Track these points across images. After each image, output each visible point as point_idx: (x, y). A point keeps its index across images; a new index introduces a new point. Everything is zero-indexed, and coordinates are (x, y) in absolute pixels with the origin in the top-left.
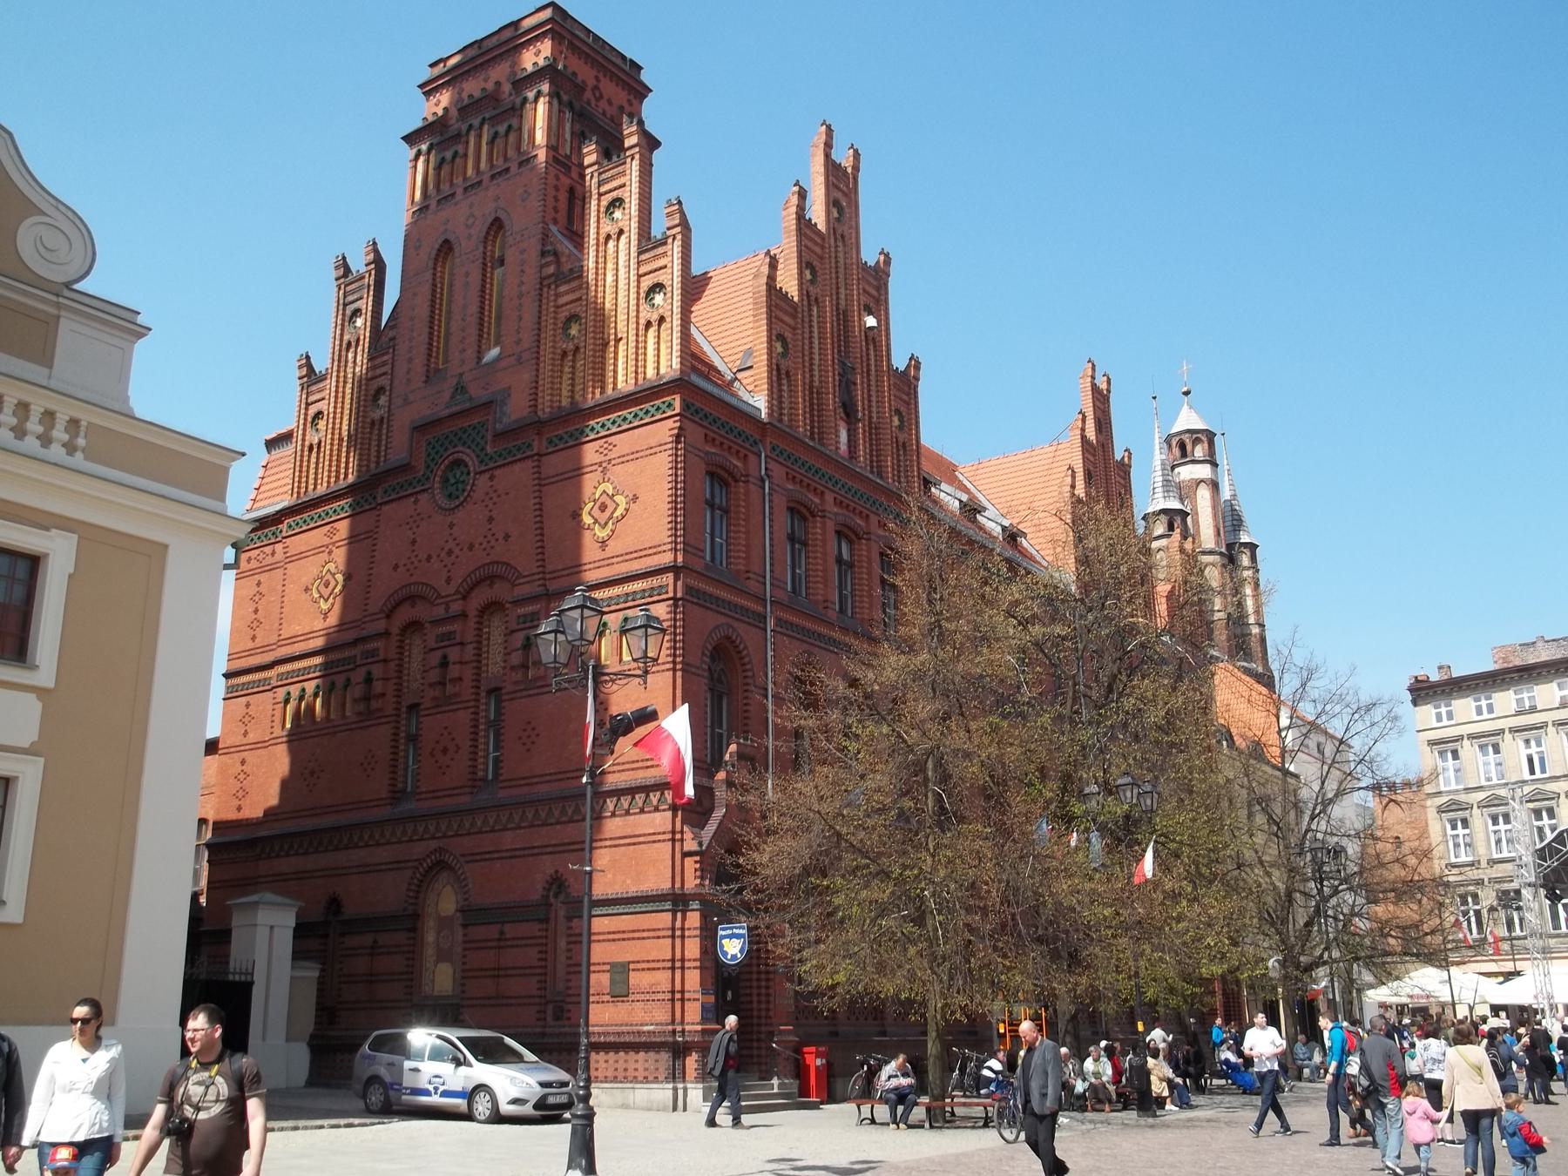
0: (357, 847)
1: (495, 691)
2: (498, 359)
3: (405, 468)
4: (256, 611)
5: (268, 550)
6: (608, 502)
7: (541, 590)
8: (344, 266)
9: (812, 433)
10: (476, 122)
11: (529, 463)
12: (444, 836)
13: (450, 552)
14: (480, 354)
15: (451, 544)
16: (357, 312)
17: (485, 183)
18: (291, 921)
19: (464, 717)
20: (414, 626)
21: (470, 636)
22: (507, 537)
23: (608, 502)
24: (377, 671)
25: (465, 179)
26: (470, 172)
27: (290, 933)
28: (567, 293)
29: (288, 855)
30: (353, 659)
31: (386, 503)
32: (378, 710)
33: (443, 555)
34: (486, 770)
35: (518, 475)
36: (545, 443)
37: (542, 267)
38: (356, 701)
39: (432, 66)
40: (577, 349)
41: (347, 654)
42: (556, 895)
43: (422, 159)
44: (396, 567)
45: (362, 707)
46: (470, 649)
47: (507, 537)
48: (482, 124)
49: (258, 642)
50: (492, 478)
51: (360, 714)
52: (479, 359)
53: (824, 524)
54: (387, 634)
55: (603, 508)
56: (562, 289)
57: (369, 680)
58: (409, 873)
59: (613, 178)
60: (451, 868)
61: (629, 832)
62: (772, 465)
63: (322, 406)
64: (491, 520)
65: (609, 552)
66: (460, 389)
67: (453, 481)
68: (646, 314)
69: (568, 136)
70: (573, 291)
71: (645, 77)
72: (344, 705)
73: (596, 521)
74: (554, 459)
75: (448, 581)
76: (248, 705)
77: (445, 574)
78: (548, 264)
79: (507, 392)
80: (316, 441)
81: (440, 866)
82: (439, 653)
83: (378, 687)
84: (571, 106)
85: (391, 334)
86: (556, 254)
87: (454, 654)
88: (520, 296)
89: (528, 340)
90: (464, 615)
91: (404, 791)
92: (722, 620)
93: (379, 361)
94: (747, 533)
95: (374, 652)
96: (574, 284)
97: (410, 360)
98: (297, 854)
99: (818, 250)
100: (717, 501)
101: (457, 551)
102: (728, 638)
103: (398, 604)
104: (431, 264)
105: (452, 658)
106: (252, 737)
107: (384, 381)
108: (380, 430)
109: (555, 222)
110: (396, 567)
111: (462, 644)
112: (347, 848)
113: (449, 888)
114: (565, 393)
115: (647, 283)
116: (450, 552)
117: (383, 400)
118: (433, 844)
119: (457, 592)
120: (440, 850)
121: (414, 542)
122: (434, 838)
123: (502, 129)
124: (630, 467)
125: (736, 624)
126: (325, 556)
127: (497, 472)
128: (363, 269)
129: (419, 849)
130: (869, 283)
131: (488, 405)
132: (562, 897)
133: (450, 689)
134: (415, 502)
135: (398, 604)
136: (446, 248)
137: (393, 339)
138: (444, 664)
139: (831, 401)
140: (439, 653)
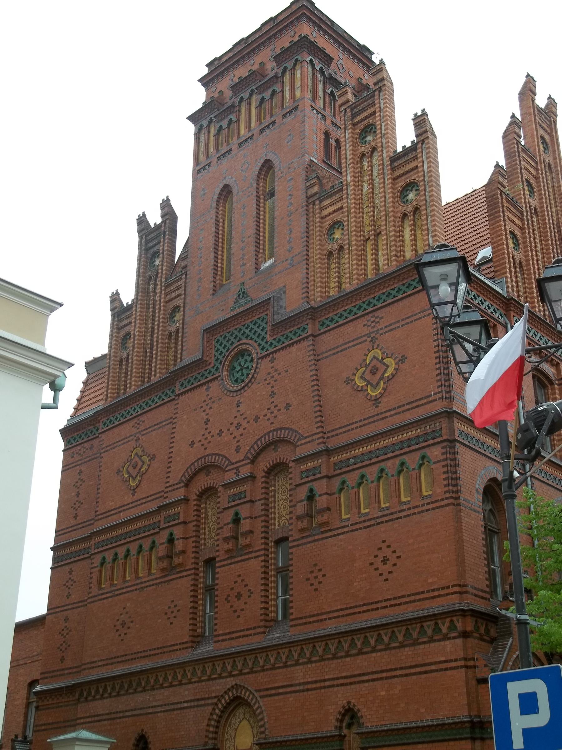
0: (162, 687)
2: (273, 266)
3: (199, 363)
4: (78, 494)
5: (87, 445)
6: (379, 365)
7: (322, 447)
10: (246, 95)
12: (241, 673)
13: (238, 426)
16: (156, 255)
19: (256, 565)
20: (208, 492)
21: (259, 494)
22: (288, 406)
23: (379, 365)
24: (178, 532)
26: (242, 132)
28: (330, 205)
29: (102, 698)
31: (182, 394)
32: (181, 565)
33: (233, 428)
34: (277, 612)
36: (318, 326)
37: (307, 188)
38: (160, 559)
40: (341, 248)
42: (349, 726)
43: (203, 132)
44: (193, 443)
45: (165, 564)
46: (259, 506)
47: (288, 406)
49: (79, 520)
51: (163, 570)
55: (374, 371)
56: (325, 203)
57: (171, 541)
60: (248, 704)
61: (420, 660)
63: (131, 328)
64: (273, 394)
65: (383, 407)
66: (243, 294)
67: (238, 368)
68: (402, 209)
72: (150, 564)
73: (368, 383)
74: (325, 338)
75: (237, 451)
76: (71, 572)
77: (234, 444)
79: (283, 291)
80: (125, 355)
81: (237, 702)
83: (179, 545)
85: (183, 264)
87: (244, 511)
91: (202, 636)
97: (200, 280)
98: (110, 696)
101: (244, 424)
103: (195, 474)
104: (214, 205)
105: (242, 515)
106: (74, 598)
107: (179, 301)
108: (176, 339)
110: (193, 443)
111: (251, 501)
112: (153, 689)
113: (245, 722)
114: (332, 285)
115: (401, 183)
116: (238, 426)
117: (178, 317)
118: (231, 682)
119: (246, 457)
120: (236, 686)
121: (207, 422)
122: (230, 675)
123: (267, 95)
126: (133, 443)
128: (159, 221)
131: (266, 303)
132: (355, 729)
133: (243, 541)
134: (207, 390)
135: (195, 474)
136: (226, 192)
137: (186, 267)
138: (237, 520)
140: (232, 512)
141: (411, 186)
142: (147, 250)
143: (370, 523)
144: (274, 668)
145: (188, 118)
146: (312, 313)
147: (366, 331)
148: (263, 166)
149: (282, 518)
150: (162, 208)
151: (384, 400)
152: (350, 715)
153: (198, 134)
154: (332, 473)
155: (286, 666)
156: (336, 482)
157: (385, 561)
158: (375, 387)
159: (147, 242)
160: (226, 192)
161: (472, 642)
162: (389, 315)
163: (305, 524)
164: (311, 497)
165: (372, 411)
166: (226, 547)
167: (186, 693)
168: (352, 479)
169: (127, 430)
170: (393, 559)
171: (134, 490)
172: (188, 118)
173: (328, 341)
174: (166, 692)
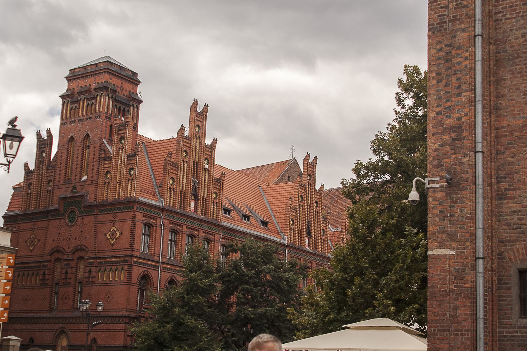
0: (39, 323)
1: (80, 283)
9: (180, 207)
11: (93, 217)
12: (64, 323)
14: (81, 178)
15: (70, 237)
16: (44, 151)
17: (85, 120)
18: (19, 344)
22: (86, 238)
25: (79, 117)
26: (80, 114)
27: (19, 348)
30: (39, 267)
31: (52, 220)
35: (90, 220)
39: (70, 70)
41: (38, 265)
42: (94, 343)
44: (53, 241)
45: (42, 282)
46: (74, 270)
48: (85, 99)
50: (83, 219)
51: (41, 284)
52: (81, 179)
53: (182, 235)
54: (50, 261)
55: (113, 234)
56: (106, 162)
57: (44, 274)
58: (54, 333)
59: (122, 130)
61: (113, 328)
62: (165, 221)
64: (82, 232)
68: (128, 177)
69: (111, 107)
70: (108, 164)
71: (140, 78)
72: (36, 280)
75: (69, 248)
78: (102, 154)
81: (63, 332)
82: (65, 269)
83: (47, 277)
84: (112, 97)
85: (54, 163)
86: (104, 151)
87: (69, 271)
88: (93, 162)
89: (95, 178)
92: (145, 269)
93: (50, 171)
94: (155, 242)
95: (46, 266)
96: (109, 162)
98: (21, 323)
99: (189, 145)
102: (146, 274)
103: (54, 252)
105: (69, 272)
107: (52, 178)
109: (105, 138)
110: (53, 241)
112: (36, 323)
116: (70, 239)
117: (51, 184)
118: (61, 325)
119: (71, 252)
120: (63, 327)
121: (59, 234)
122: (61, 323)
124: (121, 224)
125: (149, 270)
127: (84, 217)
128: (46, 138)
129: (57, 326)
130: (208, 151)
132: (95, 345)
135: (54, 252)
136: (72, 139)
139: (189, 195)
140: (65, 269)
141: (132, 169)
142: (40, 148)
143: (106, 284)
144: (74, 323)
145: (61, 97)
146: (97, 206)
147: (112, 219)
148: (86, 136)
149: (81, 275)
150: (47, 133)
151: (114, 245)
152: (94, 340)
153: (63, 105)
154: (97, 265)
155: (78, 323)
156: (98, 268)
157: (109, 297)
158: (113, 240)
159: (40, 145)
162: (120, 216)
163: (87, 280)
164: (90, 271)
165: (110, 248)
166: (63, 281)
167: (47, 326)
168: (103, 269)
169: (29, 226)
170: (111, 297)
171: (31, 251)
173: (101, 218)
174: (40, 325)
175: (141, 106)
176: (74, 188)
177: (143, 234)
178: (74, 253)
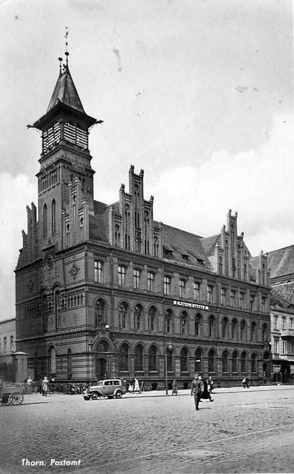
8: (28, 207)
11: (61, 260)
46: (54, 301)
71: (91, 154)
75: (50, 286)
90: (53, 294)
100: (99, 267)
105: (51, 303)
136: (45, 205)
146: (63, 252)
152: (69, 350)
160: (45, 205)
161: (88, 337)
172: (36, 175)
173: (67, 260)
175: (95, 176)
176: (49, 241)
177: (96, 268)
178: (53, 289)
